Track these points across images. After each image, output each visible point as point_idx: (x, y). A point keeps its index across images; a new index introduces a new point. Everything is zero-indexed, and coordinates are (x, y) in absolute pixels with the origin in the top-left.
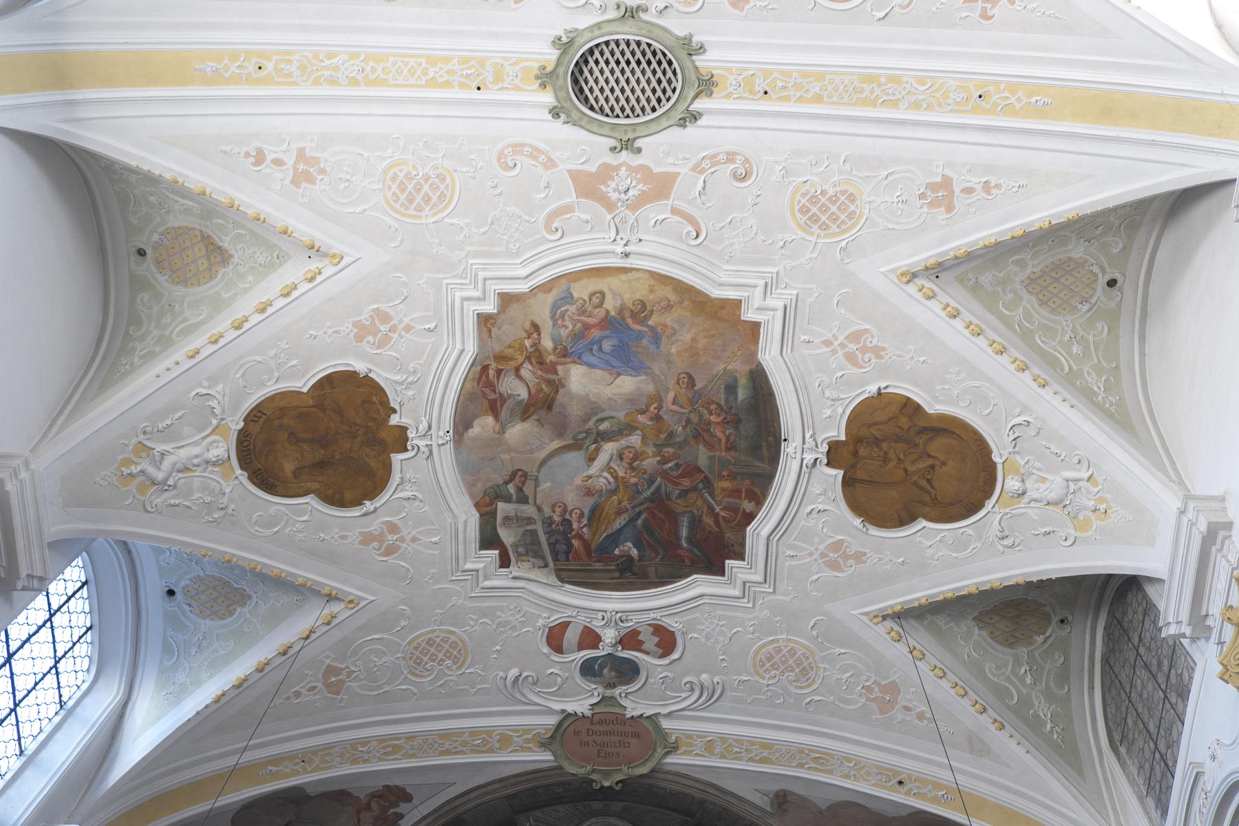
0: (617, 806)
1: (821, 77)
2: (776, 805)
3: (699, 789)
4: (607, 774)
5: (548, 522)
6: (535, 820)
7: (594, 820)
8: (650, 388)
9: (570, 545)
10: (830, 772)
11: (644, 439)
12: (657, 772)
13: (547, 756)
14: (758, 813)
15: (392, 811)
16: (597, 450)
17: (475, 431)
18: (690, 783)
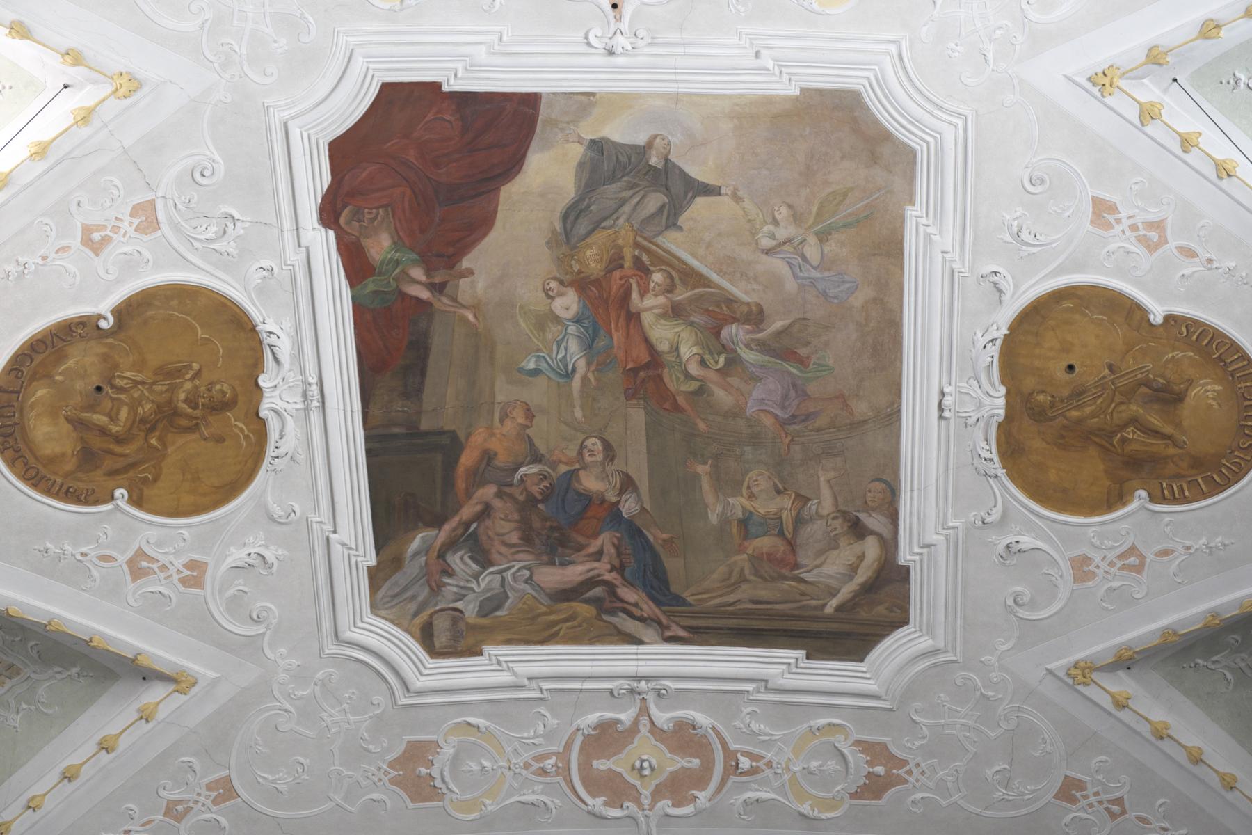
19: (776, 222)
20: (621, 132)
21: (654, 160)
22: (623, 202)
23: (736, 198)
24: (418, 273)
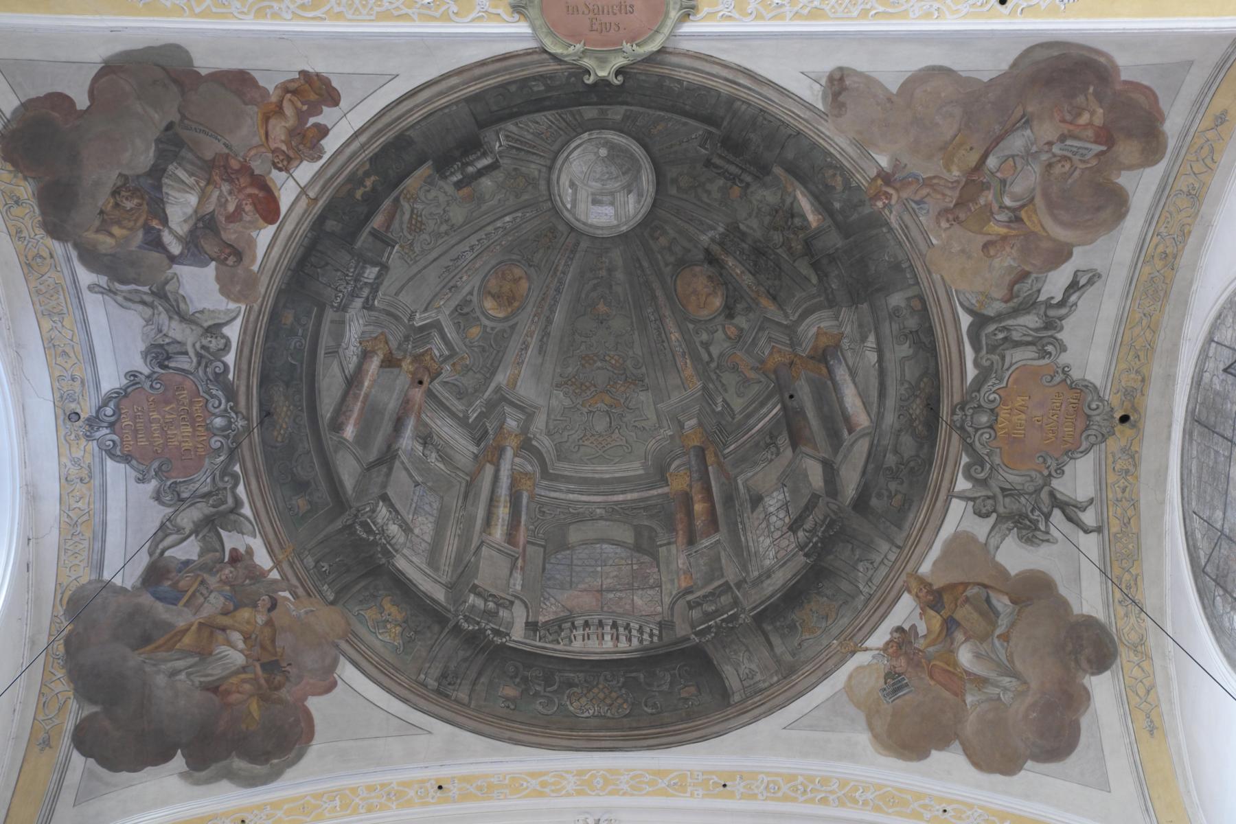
0: (617, 113)
2: (830, 96)
3: (727, 80)
4: (603, 61)
6: (507, 136)
7: (586, 136)
10: (904, 15)
12: (670, 53)
13: (523, 28)
14: (806, 114)
15: (312, 121)
18: (716, 70)
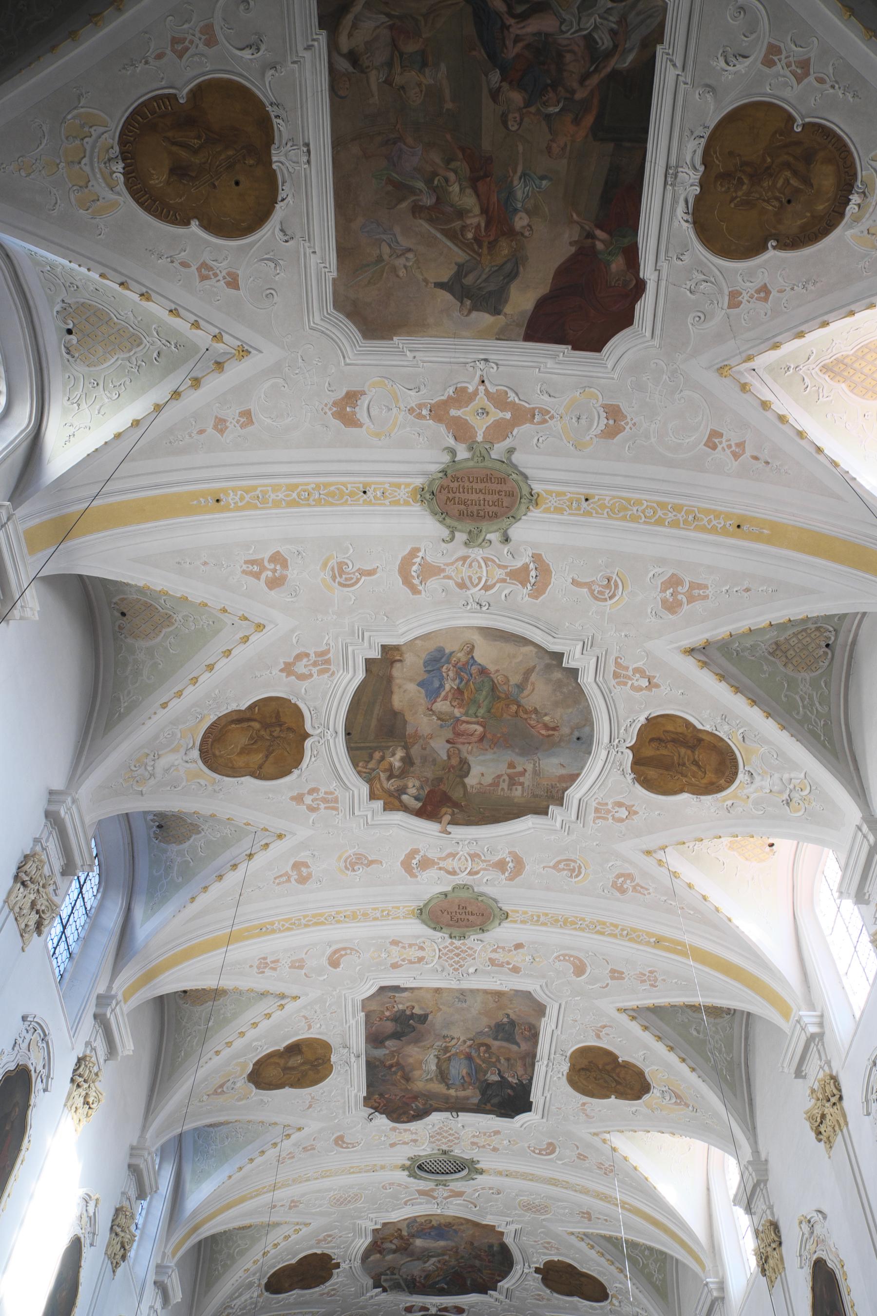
1: (533, 1175)
5: (405, 1280)
8: (453, 1244)
9: (415, 1285)
11: (450, 1257)
16: (428, 1260)
17: (372, 1258)
19: (405, 267)
20: (485, 319)
21: (468, 303)
22: (486, 280)
23: (426, 281)
24: (600, 246)
